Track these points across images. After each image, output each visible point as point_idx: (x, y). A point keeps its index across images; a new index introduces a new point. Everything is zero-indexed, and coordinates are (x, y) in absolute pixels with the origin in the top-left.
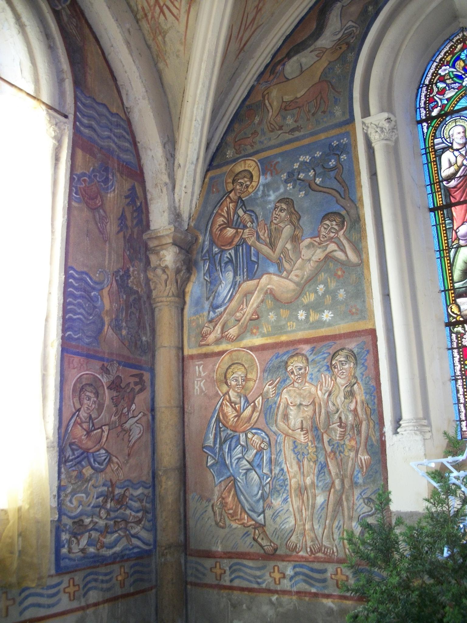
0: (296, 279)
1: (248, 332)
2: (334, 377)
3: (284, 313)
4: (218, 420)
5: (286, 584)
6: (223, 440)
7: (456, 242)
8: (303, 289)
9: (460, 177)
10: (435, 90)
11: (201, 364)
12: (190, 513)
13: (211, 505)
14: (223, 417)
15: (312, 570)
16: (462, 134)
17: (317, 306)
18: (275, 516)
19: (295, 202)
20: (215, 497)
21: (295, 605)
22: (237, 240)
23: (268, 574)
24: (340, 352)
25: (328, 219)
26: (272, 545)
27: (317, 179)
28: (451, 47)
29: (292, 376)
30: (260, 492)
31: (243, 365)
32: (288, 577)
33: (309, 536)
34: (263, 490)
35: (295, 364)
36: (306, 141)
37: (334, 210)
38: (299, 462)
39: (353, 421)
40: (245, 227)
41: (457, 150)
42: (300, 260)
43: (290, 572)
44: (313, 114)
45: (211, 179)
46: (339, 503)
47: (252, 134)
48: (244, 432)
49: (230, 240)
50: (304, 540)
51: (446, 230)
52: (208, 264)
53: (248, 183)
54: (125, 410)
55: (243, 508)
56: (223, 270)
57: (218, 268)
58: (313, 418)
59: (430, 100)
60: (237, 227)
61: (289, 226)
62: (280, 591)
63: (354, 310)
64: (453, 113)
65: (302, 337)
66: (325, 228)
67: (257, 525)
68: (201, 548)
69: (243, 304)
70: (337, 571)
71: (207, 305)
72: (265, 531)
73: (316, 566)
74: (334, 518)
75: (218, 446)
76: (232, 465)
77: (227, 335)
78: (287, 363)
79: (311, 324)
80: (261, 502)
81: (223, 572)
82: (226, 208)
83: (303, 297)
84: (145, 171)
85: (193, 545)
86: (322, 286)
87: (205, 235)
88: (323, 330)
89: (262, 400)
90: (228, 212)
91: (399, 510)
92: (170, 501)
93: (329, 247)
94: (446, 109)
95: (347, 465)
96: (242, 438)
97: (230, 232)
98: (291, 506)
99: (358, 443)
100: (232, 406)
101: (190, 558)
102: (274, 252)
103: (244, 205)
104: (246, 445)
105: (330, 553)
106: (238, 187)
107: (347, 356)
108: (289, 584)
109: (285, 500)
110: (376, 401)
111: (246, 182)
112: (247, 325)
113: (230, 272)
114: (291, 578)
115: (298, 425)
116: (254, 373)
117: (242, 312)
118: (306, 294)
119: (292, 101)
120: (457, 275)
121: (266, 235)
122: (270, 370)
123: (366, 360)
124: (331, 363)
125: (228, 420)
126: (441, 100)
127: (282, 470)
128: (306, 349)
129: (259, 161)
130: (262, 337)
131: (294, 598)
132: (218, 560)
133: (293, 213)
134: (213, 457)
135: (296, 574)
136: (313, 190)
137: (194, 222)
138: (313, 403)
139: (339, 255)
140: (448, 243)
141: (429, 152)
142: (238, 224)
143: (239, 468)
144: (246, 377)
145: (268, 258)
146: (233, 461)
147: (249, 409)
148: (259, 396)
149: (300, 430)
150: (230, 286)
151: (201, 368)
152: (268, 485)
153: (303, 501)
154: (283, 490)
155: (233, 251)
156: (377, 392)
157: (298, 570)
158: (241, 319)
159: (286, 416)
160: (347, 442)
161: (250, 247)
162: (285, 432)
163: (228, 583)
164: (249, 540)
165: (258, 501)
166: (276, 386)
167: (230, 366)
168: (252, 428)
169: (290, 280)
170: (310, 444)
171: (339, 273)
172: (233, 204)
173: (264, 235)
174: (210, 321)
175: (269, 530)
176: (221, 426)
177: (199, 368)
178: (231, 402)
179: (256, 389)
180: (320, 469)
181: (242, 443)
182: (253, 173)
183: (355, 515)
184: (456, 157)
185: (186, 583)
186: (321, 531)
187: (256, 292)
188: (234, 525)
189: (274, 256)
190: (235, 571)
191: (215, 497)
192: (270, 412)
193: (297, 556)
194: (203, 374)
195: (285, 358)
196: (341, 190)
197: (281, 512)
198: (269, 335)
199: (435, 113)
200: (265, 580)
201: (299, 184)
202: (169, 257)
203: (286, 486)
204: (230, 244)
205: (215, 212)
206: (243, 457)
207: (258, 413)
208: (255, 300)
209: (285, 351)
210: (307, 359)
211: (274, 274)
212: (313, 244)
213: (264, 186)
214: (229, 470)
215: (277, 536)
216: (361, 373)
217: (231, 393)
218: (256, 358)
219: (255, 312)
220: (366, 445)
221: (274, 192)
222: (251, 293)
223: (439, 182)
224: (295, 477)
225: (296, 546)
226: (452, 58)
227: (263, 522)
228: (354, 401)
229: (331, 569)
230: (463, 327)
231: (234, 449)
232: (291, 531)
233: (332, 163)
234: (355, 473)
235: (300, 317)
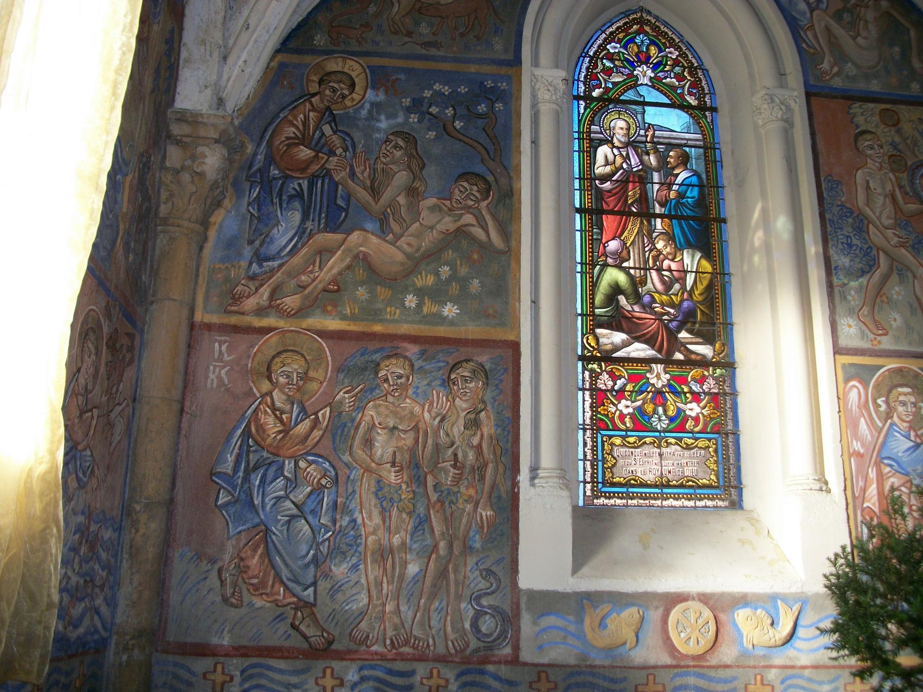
0: (408, 249)
1: (318, 307)
2: (451, 397)
3: (383, 293)
4: (247, 434)
6: (251, 465)
7: (603, 258)
8: (417, 265)
9: (617, 181)
10: (600, 67)
11: (225, 342)
13: (217, 567)
14: (257, 431)
15: (390, 672)
16: (625, 132)
17: (438, 294)
18: (335, 590)
19: (419, 143)
20: (227, 557)
22: (315, 168)
23: (312, 681)
24: (464, 364)
25: (467, 181)
26: (325, 634)
27: (457, 122)
28: (625, 24)
29: (386, 385)
30: (312, 552)
31: (303, 356)
32: (348, 685)
33: (390, 622)
34: (318, 549)
35: (393, 369)
36: (447, 66)
37: (477, 171)
38: (384, 512)
39: (474, 461)
40: (332, 153)
41: (618, 148)
42: (417, 224)
44: (462, 35)
45: (282, 65)
46: (443, 574)
47: (362, 25)
48: (292, 457)
49: (303, 166)
50: (382, 627)
51: (592, 240)
52: (258, 190)
53: (346, 92)
54: (115, 389)
55: (278, 576)
56: (284, 205)
57: (276, 201)
58: (413, 451)
59: (591, 77)
60: (317, 149)
61: (405, 173)
63: (491, 311)
64: (617, 101)
65: (407, 332)
66: (461, 191)
67: (301, 604)
68: (189, 640)
69: (314, 264)
70: (431, 673)
71: (248, 252)
72: (313, 613)
73: (399, 666)
74: (433, 596)
75: (241, 474)
76: (263, 507)
77: (280, 305)
78: (378, 365)
79: (424, 317)
80: (312, 567)
81: (228, 679)
82: (302, 116)
83: (416, 277)
84: (187, 12)
85: (172, 636)
86: (447, 268)
87: (259, 145)
88: (442, 329)
89: (330, 412)
90: (305, 123)
91: (531, 587)
93: (464, 217)
94: (610, 94)
95: (460, 523)
96: (289, 466)
97: (305, 153)
98: (363, 576)
99: (479, 491)
100: (276, 415)
102: (376, 203)
103: (335, 121)
104: (293, 479)
105: (422, 647)
106: (327, 92)
107: (474, 371)
109: (355, 567)
110: (510, 438)
111: (342, 89)
112: (317, 297)
113: (297, 212)
114: (354, 685)
115: (388, 457)
116: (320, 371)
117: (312, 276)
118: (421, 274)
119: (431, 5)
120: (599, 298)
121: (366, 174)
122: (349, 370)
123: (501, 381)
124: (449, 377)
125: (265, 436)
126: (606, 81)
127: (354, 521)
128: (412, 350)
129: (368, 67)
130: (341, 319)
132: (222, 659)
133: (414, 157)
134: (229, 492)
135: (363, 679)
136: (448, 134)
137: (240, 119)
138: (416, 429)
139: (478, 232)
140: (592, 257)
141: (583, 139)
142: (320, 145)
143: (278, 513)
144: (306, 374)
145: (365, 208)
146: (267, 500)
147: (307, 424)
148: (325, 407)
149: (389, 465)
150: (294, 231)
151: (224, 348)
152: (327, 543)
153: (385, 570)
154: (352, 551)
155: (306, 182)
156: (513, 427)
157: (366, 672)
158: (308, 285)
159: (368, 443)
160: (463, 490)
161: (336, 185)
162: (364, 465)
164: (283, 627)
165: (307, 565)
166: (356, 395)
167: (279, 353)
168: (308, 454)
169: (397, 247)
170: (404, 486)
171: (475, 256)
172: (316, 114)
173: (363, 173)
174: (252, 278)
175: (321, 612)
176: (251, 444)
177: (220, 347)
178: (274, 409)
179: (321, 395)
180: (416, 524)
181: (286, 474)
182: (356, 80)
183: (467, 593)
184: (615, 156)
186: (410, 614)
187: (340, 252)
188: (258, 602)
189: (377, 207)
190: (251, 677)
192: (342, 432)
194: (226, 358)
195: (377, 357)
196: (490, 147)
197: (346, 585)
198: (353, 318)
199: (596, 93)
201: (429, 120)
202: (212, 160)
203: (358, 546)
204: (303, 170)
205: (282, 115)
206: (287, 497)
207: (321, 432)
208: (335, 264)
209: (378, 346)
210: (412, 365)
211: (373, 233)
212: (440, 207)
213: (372, 104)
214: (258, 514)
215: (335, 621)
216: (493, 398)
217: (275, 394)
218: (327, 349)
219: (334, 281)
220: (490, 497)
221: (388, 118)
222: (332, 252)
223: (591, 179)
224: (374, 533)
225: (368, 636)
226: (625, 37)
227: (311, 600)
228: (479, 433)
229: (421, 670)
230: (600, 365)
231: (272, 482)
232: (361, 613)
233: (482, 108)
234: (472, 534)
235: (407, 304)
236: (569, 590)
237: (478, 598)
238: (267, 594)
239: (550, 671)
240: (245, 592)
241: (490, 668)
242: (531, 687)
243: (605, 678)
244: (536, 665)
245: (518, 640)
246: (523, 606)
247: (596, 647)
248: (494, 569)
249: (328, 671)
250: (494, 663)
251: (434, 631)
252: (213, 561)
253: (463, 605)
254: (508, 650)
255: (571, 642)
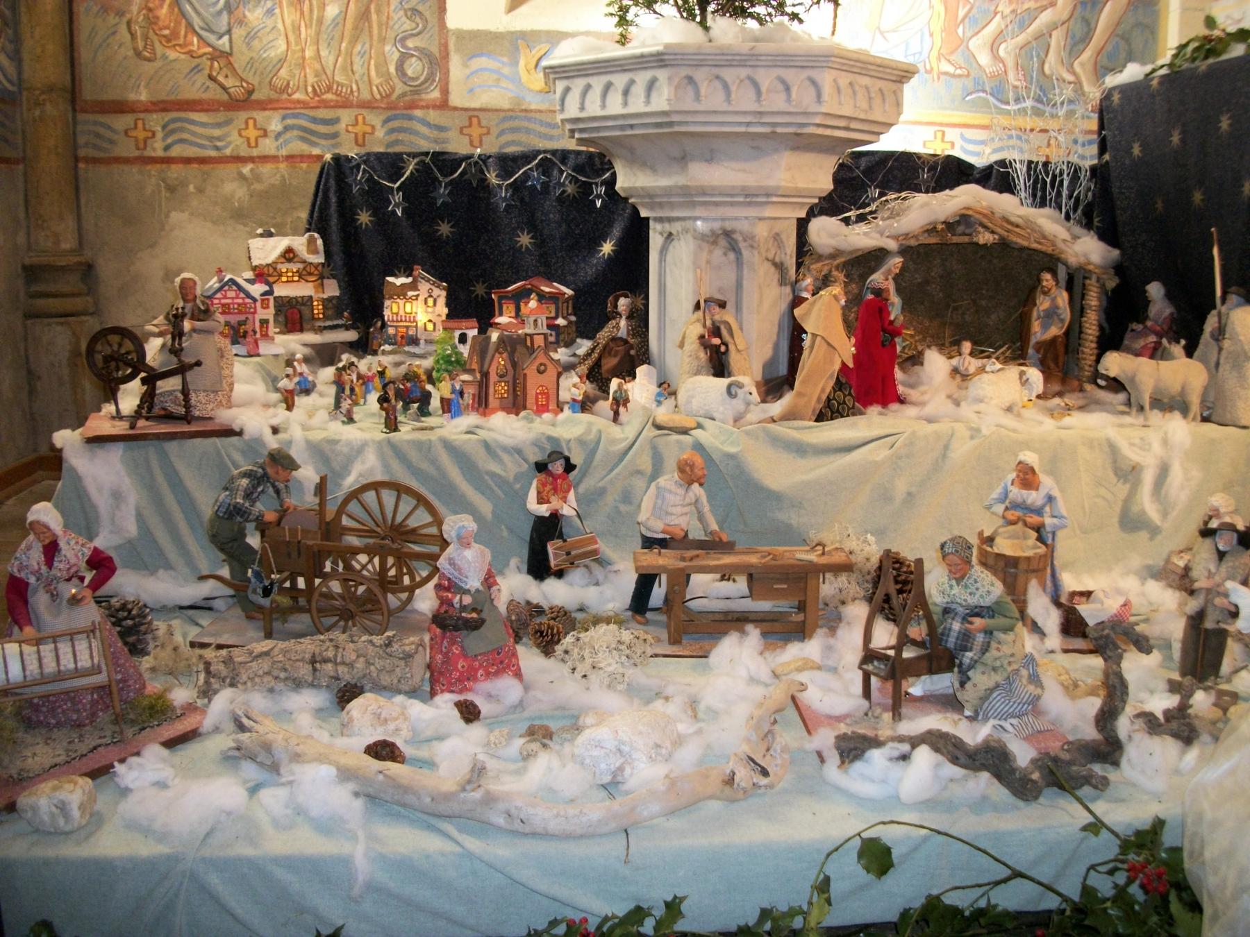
5: (268, 146)
12: (82, 37)
13: (125, 20)
15: (314, 120)
18: (251, 37)
20: (135, 9)
21: (283, 176)
32: (272, 135)
43: (275, 125)
55: (190, 26)
62: (259, 157)
67: (217, 53)
68: (105, 97)
73: (322, 113)
74: (354, 40)
80: (225, 13)
81: (150, 134)
85: (88, 93)
92: (49, 7)
101: (81, 117)
108: (276, 144)
109: (270, 12)
114: (278, 135)
131: (283, 166)
132: (142, 115)
153: (302, 13)
157: (289, 122)
163: (160, 153)
164: (201, 79)
165: (220, 13)
175: (239, 61)
183: (391, 34)
185: (77, 159)
186: (331, 59)
188: (172, 55)
190: (173, 131)
191: (135, 9)
193: (290, 101)
200: (230, 143)
227: (227, 49)
229: (346, 116)
236: (501, 29)
237: (403, 40)
238: (180, 45)
239: (481, 115)
240: (157, 45)
241: (418, 113)
242: (461, 132)
243: (541, 123)
244: (466, 110)
245: (447, 84)
246: (452, 47)
247: (532, 91)
248: (420, 8)
249: (251, 122)
250: (422, 107)
251: (357, 76)
252: (120, 14)
253: (387, 48)
254: (435, 94)
255: (504, 85)
